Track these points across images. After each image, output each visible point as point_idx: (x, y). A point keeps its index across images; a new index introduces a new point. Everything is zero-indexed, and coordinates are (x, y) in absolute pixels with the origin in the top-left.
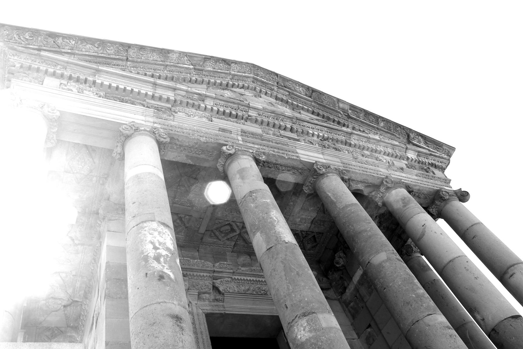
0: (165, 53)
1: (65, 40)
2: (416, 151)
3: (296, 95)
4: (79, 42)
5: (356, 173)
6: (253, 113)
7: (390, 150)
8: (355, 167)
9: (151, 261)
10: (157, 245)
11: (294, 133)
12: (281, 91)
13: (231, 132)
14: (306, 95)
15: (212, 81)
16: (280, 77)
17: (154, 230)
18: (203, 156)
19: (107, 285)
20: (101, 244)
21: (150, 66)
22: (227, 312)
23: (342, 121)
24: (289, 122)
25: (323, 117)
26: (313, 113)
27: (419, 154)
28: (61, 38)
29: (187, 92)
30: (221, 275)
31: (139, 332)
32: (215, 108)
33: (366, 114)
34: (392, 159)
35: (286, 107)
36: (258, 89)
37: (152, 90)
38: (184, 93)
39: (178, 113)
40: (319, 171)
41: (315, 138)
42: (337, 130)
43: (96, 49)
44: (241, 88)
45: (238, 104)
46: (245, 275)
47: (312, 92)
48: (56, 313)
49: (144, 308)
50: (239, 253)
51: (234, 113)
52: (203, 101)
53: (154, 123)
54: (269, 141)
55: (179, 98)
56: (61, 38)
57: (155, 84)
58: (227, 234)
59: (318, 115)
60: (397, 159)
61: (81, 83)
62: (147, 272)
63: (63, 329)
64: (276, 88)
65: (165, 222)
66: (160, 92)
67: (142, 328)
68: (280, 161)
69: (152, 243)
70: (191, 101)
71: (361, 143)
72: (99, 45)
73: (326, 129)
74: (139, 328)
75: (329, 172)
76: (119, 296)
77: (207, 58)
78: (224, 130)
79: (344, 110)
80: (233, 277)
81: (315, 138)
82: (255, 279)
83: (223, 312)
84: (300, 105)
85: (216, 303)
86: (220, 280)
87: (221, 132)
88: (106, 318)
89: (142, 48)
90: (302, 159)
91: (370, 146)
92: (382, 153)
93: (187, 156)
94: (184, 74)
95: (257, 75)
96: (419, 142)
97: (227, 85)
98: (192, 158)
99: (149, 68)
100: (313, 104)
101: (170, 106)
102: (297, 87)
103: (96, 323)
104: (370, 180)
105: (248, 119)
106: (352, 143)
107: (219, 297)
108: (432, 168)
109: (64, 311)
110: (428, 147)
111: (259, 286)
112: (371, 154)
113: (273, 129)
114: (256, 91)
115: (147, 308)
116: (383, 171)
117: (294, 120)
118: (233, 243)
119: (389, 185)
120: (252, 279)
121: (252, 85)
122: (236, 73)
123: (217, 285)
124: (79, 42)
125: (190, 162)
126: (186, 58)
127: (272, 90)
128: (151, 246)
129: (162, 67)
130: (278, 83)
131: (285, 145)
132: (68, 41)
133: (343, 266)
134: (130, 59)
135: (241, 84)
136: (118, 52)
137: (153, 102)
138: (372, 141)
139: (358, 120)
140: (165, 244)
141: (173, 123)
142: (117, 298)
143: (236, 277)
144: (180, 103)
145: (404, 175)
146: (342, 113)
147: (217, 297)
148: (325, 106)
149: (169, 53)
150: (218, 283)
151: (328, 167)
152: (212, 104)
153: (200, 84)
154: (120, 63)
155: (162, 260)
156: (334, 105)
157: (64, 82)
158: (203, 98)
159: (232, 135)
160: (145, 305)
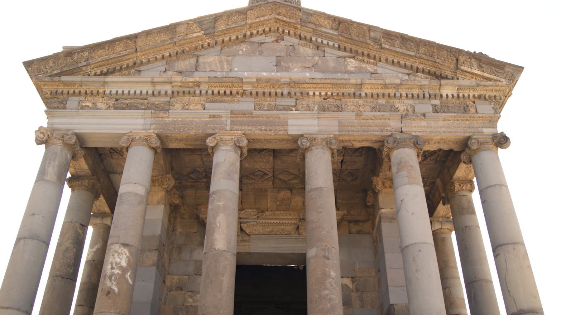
0: (172, 29)
1: (80, 54)
2: (455, 86)
3: (320, 31)
4: (92, 51)
5: (354, 136)
6: (248, 88)
7: (415, 92)
8: (353, 128)
10: (114, 266)
11: (293, 98)
12: (305, 28)
13: (221, 117)
14: (332, 28)
15: (227, 39)
16: (304, 11)
17: (116, 252)
18: (198, 143)
21: (159, 49)
22: (251, 251)
23: (372, 53)
24: (287, 87)
25: (351, 51)
26: (339, 48)
27: (460, 88)
28: (76, 54)
29: (181, 82)
30: (246, 220)
32: (210, 92)
33: (403, 40)
34: (417, 102)
35: (310, 47)
36: (281, 30)
37: (152, 88)
38: (180, 84)
39: (176, 105)
40: (301, 147)
41: (317, 98)
42: (343, 84)
43: (107, 52)
44: (262, 34)
45: (232, 82)
46: (269, 219)
47: (340, 23)
50: (280, 189)
51: (228, 92)
52: (199, 86)
53: (151, 125)
54: (260, 117)
55: (176, 89)
56: (76, 54)
57: (153, 83)
58: (262, 177)
59: (345, 50)
60: (426, 100)
61: (95, 96)
64: (299, 27)
65: (127, 243)
66: (159, 87)
68: (268, 137)
69: (112, 263)
70: (187, 90)
71: (375, 91)
72: (109, 46)
73: (330, 86)
75: (313, 146)
77: (216, 18)
78: (214, 116)
79: (375, 40)
80: (258, 221)
81: (317, 98)
82: (275, 221)
83: (248, 251)
84: (325, 42)
85: (243, 243)
86: (246, 224)
87: (211, 119)
89: (148, 33)
90: (290, 133)
91: (387, 92)
92: (403, 98)
93: (185, 144)
94: (195, 43)
95: (279, 14)
96: (471, 66)
97: (245, 36)
98: (189, 145)
99: (158, 51)
100: (340, 38)
101: (168, 99)
102: (322, 20)
104: (374, 138)
105: (243, 94)
106: (363, 94)
107: (246, 238)
108: (477, 101)
110: (483, 71)
111: (283, 227)
112: (387, 102)
113: (269, 99)
114: (279, 33)
116: (394, 124)
117: (292, 85)
118: (271, 183)
119: (389, 146)
120: (275, 221)
121: (274, 26)
122: (253, 21)
123: (244, 228)
124: (92, 51)
125: (189, 147)
126: (195, 26)
127: (296, 28)
128: (109, 267)
129: (172, 45)
130: (301, 19)
131: (277, 118)
132: (82, 54)
133: (372, 205)
134: (138, 49)
135: (260, 30)
136: (126, 48)
137: (153, 99)
138: (391, 86)
139: (391, 50)
140: (120, 263)
141: (168, 120)
143: (261, 221)
144: (178, 93)
145: (424, 123)
146: (372, 44)
147: (245, 239)
148: (352, 39)
149: (175, 28)
150: (244, 226)
151: (312, 140)
152: (207, 87)
153: (213, 47)
154: (131, 56)
155: (113, 278)
156: (364, 36)
157: (82, 98)
158: (198, 84)
159: (222, 119)
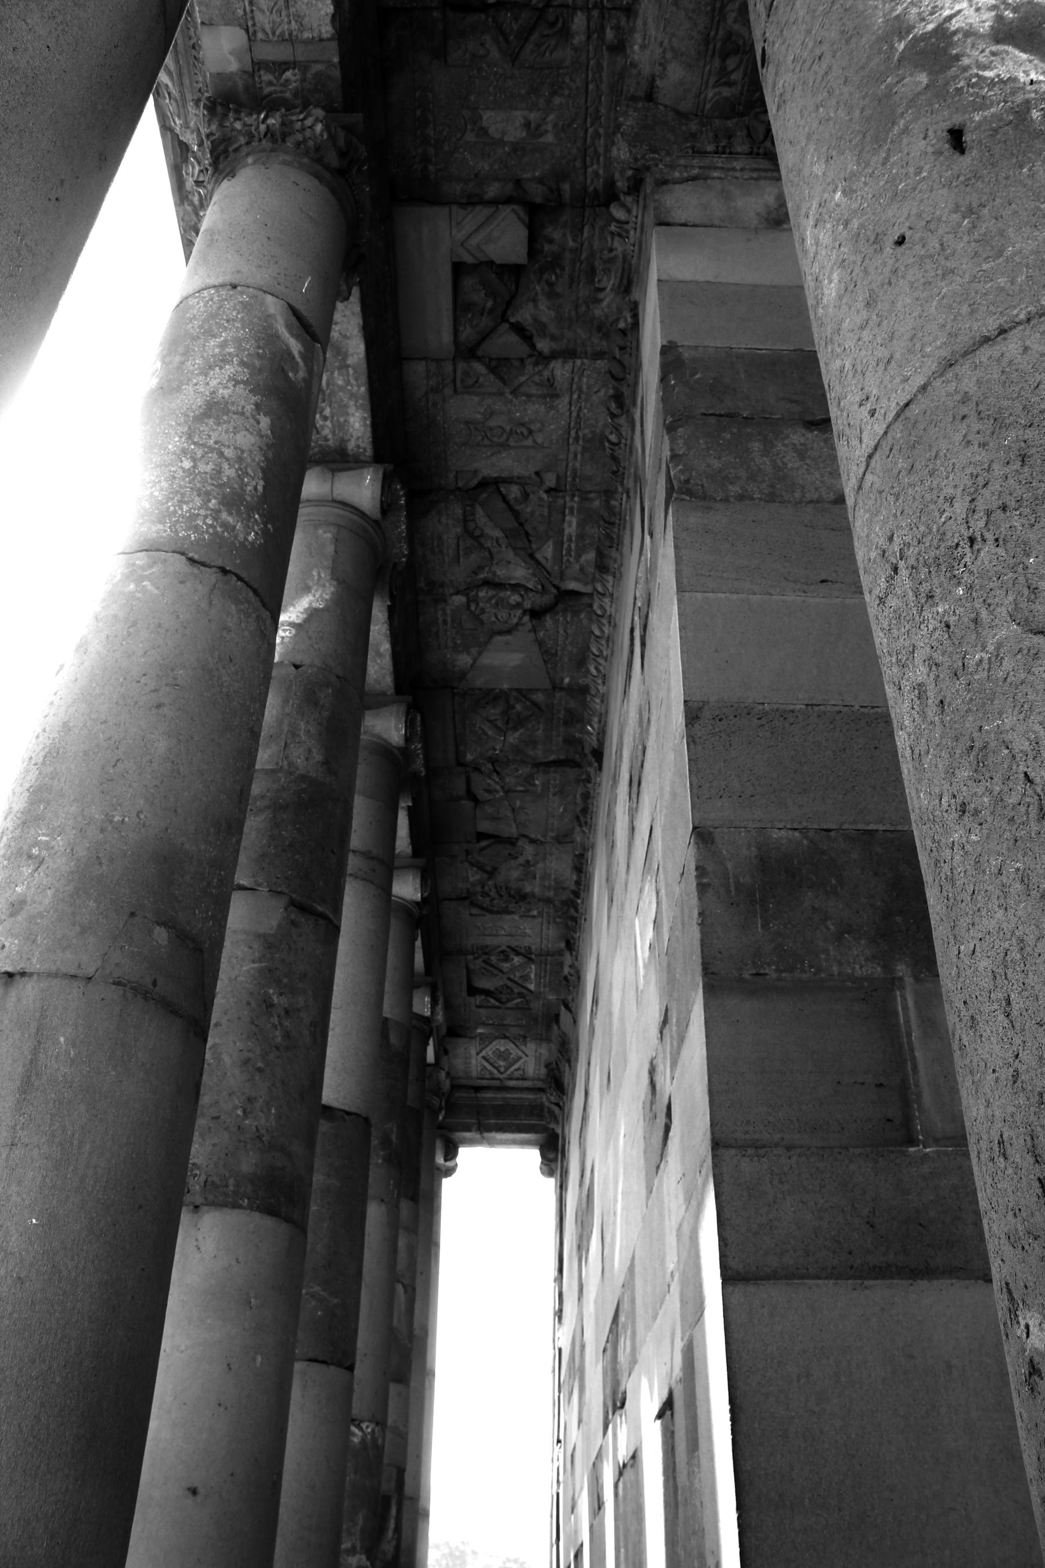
9: (973, 55)
19: (673, 441)
20: (635, 316)
31: (957, 532)
48: (509, 637)
49: (985, 354)
62: (957, 120)
63: (539, 697)
67: (987, 499)
74: (960, 508)
76: (734, 489)
88: (680, 589)
103: (643, 644)
109: (534, 630)
115: (1011, 346)
142: (726, 500)
160: (992, 324)
